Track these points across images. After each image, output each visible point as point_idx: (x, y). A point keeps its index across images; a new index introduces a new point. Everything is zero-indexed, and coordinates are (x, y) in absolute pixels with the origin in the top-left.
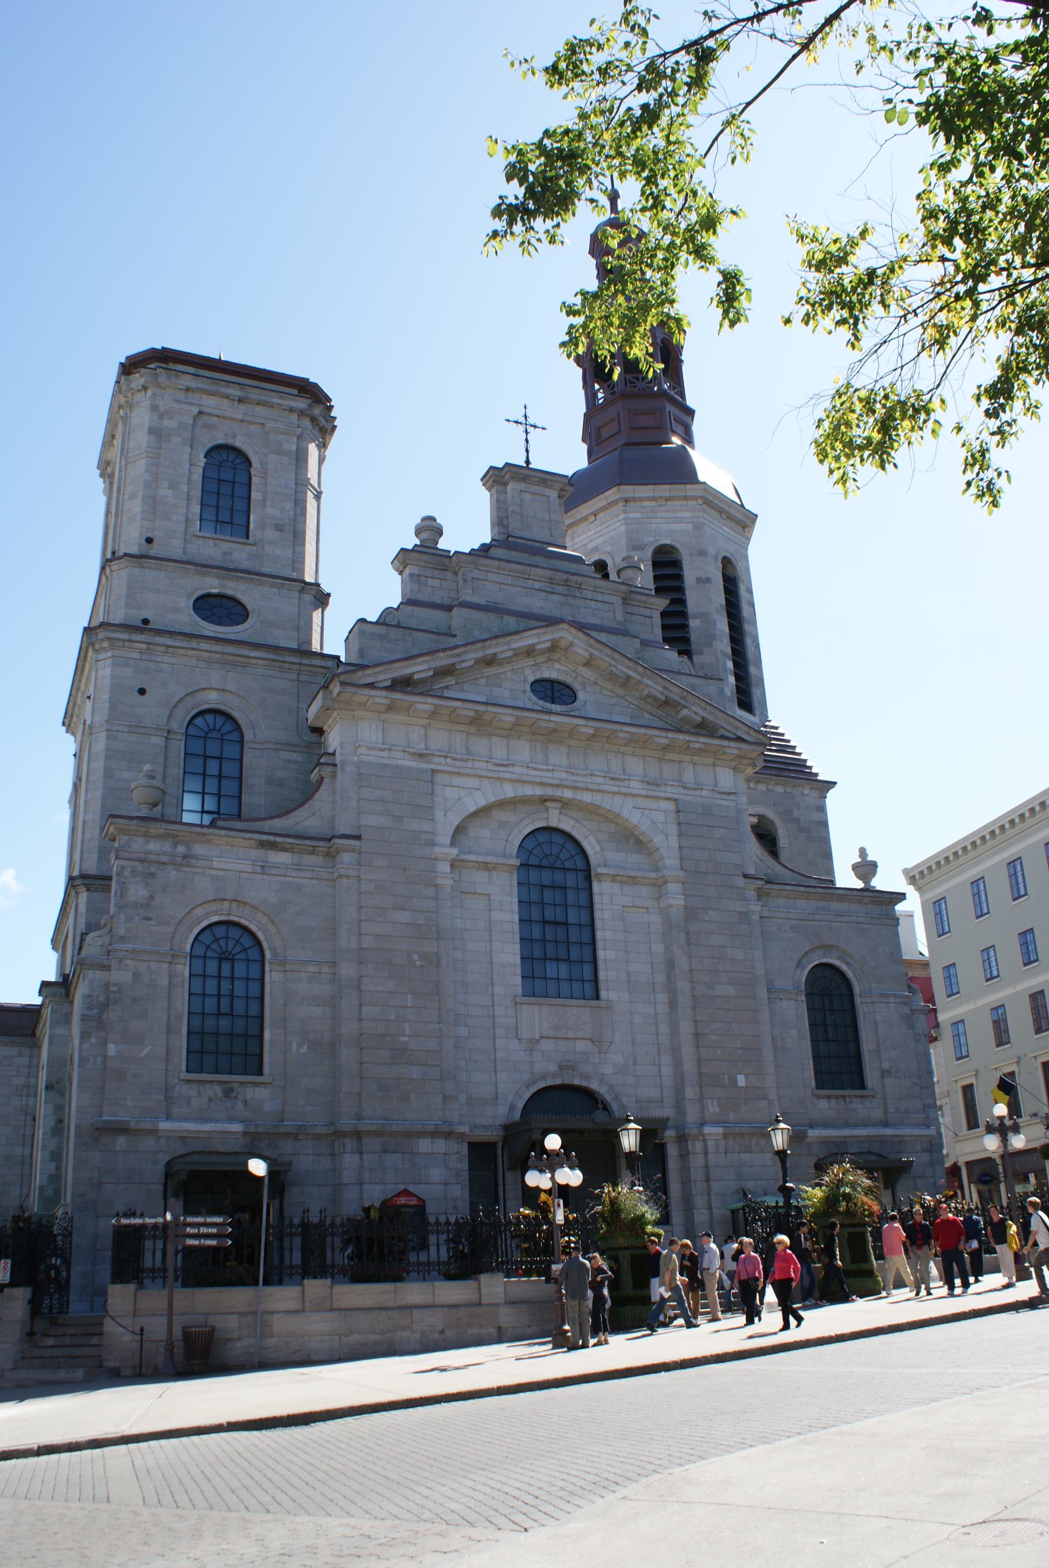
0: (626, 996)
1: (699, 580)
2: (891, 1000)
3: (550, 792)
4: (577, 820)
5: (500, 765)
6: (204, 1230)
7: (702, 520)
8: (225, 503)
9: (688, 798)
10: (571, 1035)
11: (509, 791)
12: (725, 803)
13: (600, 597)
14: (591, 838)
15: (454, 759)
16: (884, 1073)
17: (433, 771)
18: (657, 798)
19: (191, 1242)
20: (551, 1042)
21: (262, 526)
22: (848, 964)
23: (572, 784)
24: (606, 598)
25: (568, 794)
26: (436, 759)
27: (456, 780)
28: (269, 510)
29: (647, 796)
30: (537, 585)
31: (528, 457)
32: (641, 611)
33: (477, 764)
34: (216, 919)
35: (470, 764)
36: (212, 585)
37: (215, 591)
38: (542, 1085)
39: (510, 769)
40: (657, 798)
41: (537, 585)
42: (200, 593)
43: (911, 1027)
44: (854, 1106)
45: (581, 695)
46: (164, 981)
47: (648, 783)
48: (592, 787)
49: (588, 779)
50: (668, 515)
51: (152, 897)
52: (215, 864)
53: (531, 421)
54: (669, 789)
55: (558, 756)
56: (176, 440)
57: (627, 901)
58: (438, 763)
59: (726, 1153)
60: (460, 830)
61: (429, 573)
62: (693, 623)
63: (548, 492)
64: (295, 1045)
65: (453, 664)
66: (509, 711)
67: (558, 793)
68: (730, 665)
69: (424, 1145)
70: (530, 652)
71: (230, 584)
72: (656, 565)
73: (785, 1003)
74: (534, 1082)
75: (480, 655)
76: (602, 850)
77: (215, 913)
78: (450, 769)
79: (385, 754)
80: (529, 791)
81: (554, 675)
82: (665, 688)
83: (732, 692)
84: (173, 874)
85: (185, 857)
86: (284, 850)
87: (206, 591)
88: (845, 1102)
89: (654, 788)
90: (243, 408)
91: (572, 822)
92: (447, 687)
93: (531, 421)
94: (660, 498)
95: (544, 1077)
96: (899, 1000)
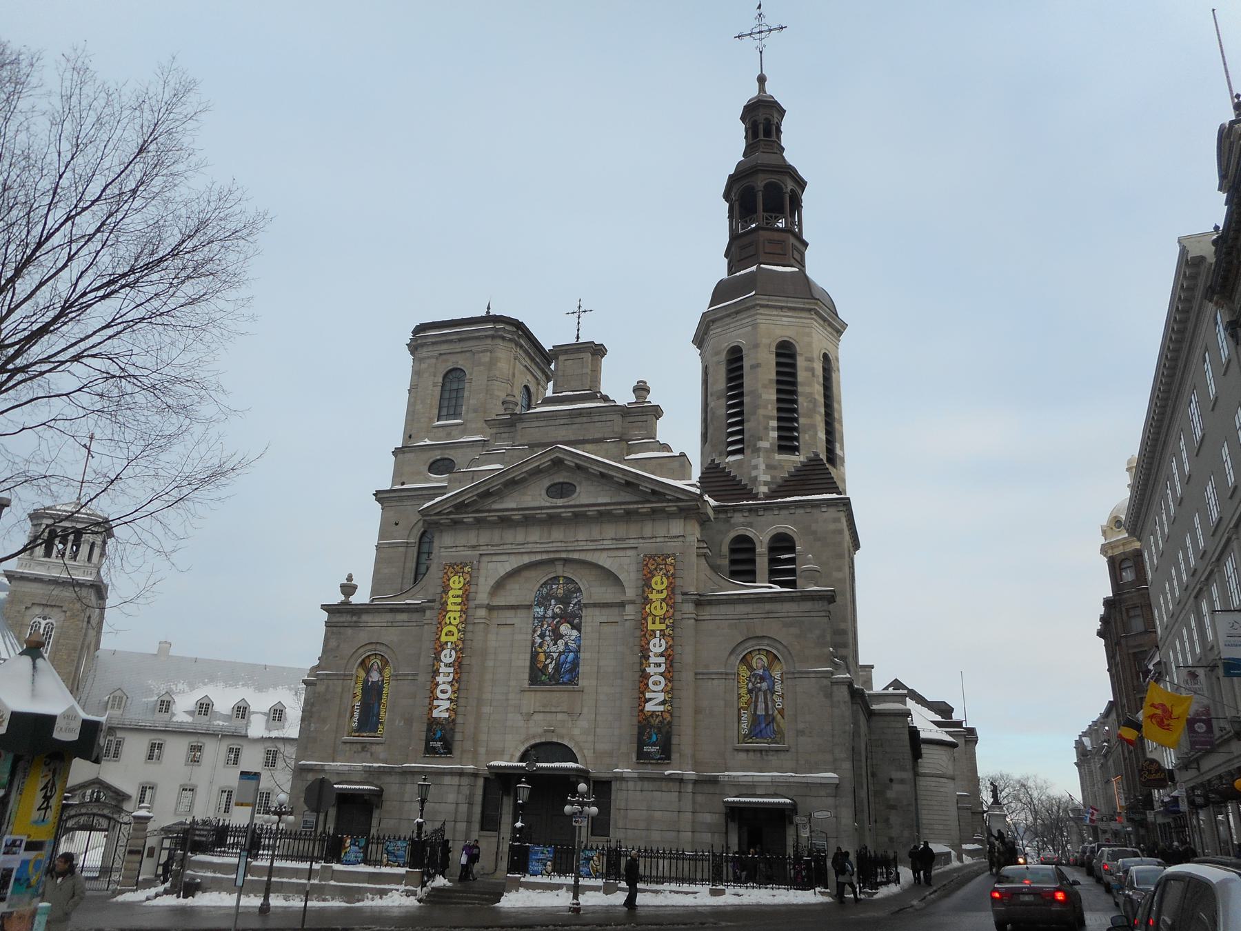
0: (594, 682)
2: (813, 675)
3: (552, 556)
5: (518, 544)
6: (202, 833)
8: (453, 402)
11: (526, 559)
13: (604, 418)
15: (493, 546)
16: (800, 733)
17: (481, 554)
19: (197, 838)
20: (542, 714)
21: (467, 412)
22: (777, 649)
23: (564, 549)
24: (609, 418)
25: (564, 555)
26: (482, 548)
27: (495, 558)
28: (471, 401)
29: (617, 549)
30: (562, 422)
31: (578, 335)
32: (640, 418)
34: (369, 653)
35: (501, 547)
36: (437, 455)
37: (439, 457)
38: (533, 742)
39: (526, 546)
41: (562, 422)
42: (431, 460)
43: (829, 695)
44: (770, 758)
45: (578, 489)
46: (339, 690)
47: (616, 540)
49: (576, 544)
50: (737, 324)
51: (338, 646)
52: (369, 624)
53: (576, 309)
54: (632, 541)
55: (557, 534)
56: (426, 375)
57: (604, 619)
58: (483, 550)
60: (499, 585)
61: (502, 430)
62: (746, 399)
63: (582, 355)
64: (397, 722)
65: (489, 489)
66: (517, 513)
68: (774, 423)
69: (447, 780)
70: (537, 472)
71: (447, 452)
72: (730, 362)
73: (715, 682)
74: (527, 740)
75: (502, 480)
78: (492, 552)
79: (454, 549)
80: (538, 557)
81: (561, 480)
83: (771, 444)
84: (349, 631)
85: (355, 622)
88: (762, 754)
90: (462, 344)
92: (494, 502)
93: (576, 309)
94: (732, 313)
95: (534, 737)
96: (819, 675)
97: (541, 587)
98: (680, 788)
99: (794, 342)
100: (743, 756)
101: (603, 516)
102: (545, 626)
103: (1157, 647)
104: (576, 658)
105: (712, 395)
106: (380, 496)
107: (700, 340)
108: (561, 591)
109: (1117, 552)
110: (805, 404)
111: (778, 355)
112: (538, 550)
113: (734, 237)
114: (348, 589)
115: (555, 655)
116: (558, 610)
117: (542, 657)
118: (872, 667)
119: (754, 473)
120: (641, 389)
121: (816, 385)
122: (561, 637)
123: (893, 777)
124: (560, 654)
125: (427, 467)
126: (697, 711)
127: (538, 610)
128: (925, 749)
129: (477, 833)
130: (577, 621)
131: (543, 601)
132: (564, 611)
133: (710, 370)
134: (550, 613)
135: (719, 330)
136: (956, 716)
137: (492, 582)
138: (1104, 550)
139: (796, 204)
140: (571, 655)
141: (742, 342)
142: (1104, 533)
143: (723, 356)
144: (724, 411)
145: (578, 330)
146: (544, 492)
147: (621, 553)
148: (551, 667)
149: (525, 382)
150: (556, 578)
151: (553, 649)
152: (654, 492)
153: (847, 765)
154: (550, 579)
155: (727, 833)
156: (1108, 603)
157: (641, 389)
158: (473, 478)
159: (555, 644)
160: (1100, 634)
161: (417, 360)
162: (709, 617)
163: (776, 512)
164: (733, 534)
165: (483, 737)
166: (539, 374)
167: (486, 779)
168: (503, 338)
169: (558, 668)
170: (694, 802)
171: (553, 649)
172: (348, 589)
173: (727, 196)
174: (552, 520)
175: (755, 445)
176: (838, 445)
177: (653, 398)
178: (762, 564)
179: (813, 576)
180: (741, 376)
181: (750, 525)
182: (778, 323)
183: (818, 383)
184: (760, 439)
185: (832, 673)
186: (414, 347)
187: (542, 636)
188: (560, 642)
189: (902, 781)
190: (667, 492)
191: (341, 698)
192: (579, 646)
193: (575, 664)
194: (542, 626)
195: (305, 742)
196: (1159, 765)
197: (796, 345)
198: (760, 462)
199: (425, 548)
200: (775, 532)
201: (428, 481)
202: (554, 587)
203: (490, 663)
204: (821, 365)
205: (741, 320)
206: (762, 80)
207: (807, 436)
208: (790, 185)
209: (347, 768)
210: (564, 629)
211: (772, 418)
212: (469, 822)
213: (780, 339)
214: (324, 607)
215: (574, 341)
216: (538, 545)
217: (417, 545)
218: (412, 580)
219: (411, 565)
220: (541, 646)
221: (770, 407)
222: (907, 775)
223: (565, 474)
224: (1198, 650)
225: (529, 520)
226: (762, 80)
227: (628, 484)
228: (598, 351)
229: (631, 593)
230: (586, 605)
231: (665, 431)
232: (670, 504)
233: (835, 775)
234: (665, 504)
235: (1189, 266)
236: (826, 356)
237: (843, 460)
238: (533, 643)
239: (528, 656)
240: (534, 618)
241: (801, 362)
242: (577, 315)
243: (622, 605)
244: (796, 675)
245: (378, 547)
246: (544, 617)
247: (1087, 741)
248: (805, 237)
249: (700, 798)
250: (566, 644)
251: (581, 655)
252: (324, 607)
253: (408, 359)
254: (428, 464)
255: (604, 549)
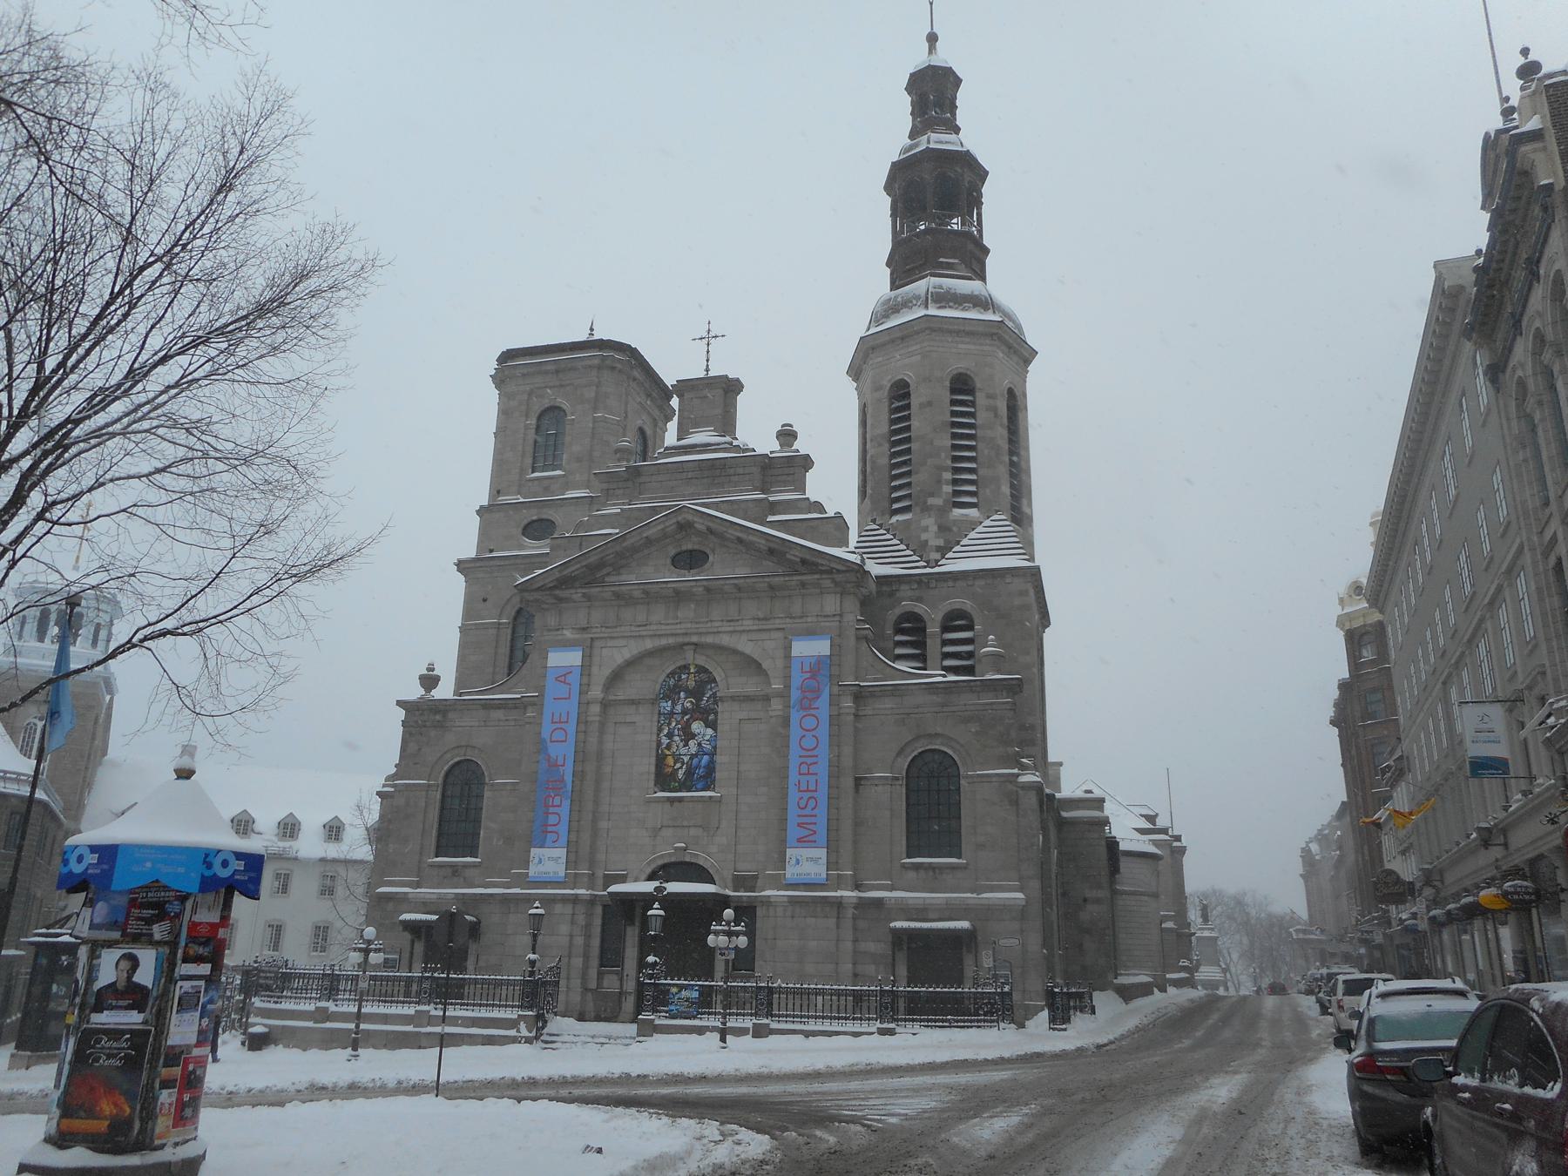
1: (922, 406)
3: (680, 640)
4: (707, 656)
5: (639, 626)
7: (928, 349)
9: (794, 626)
10: (685, 823)
11: (649, 644)
12: (827, 624)
14: (719, 669)
15: (607, 627)
17: (592, 638)
18: (770, 630)
20: (671, 830)
22: (952, 748)
23: (696, 631)
25: (695, 639)
26: (594, 630)
27: (610, 643)
29: (760, 630)
33: (623, 629)
35: (618, 629)
37: (535, 518)
39: (648, 627)
40: (770, 630)
42: (526, 522)
45: (711, 558)
48: (710, 630)
51: (420, 749)
53: (705, 334)
54: (777, 621)
55: (687, 612)
57: (744, 715)
59: (793, 917)
60: (616, 677)
62: (914, 446)
65: (602, 558)
67: (687, 640)
73: (880, 788)
76: (726, 676)
77: (457, 755)
80: (664, 642)
81: (690, 547)
82: (767, 540)
84: (433, 733)
86: (499, 708)
87: (529, 520)
89: (764, 622)
91: (704, 658)
92: (608, 574)
93: (705, 334)
96: (1002, 779)
97: (668, 676)
98: (838, 913)
99: (972, 375)
100: (911, 875)
101: (741, 591)
102: (674, 724)
103: (1399, 739)
104: (712, 763)
105: (872, 440)
106: (462, 566)
107: (855, 371)
108: (691, 684)
109: (1357, 624)
110: (986, 452)
111: (953, 391)
112: (663, 632)
113: (898, 243)
114: (430, 681)
115: (686, 759)
116: (688, 705)
117: (670, 761)
118: (1061, 764)
119: (924, 536)
120: (787, 435)
121: (999, 428)
122: (693, 736)
123: (1087, 896)
124: (692, 757)
125: (520, 530)
126: (858, 823)
127: (665, 704)
128: (1124, 864)
129: (596, 970)
130: (711, 717)
131: (671, 693)
132: (697, 705)
133: (869, 410)
134: (679, 708)
135: (880, 359)
136: (1161, 822)
137: (607, 672)
138: (1340, 622)
139: (976, 201)
140: (706, 758)
141: (909, 376)
142: (1341, 601)
143: (885, 393)
144: (887, 460)
145: (708, 361)
146: (669, 561)
147: (764, 636)
148: (681, 774)
149: (639, 422)
150: (685, 668)
151: (683, 751)
152: (804, 562)
153: (1035, 884)
154: (679, 668)
155: (894, 965)
156: (1344, 686)
157: (787, 435)
158: (581, 545)
159: (686, 745)
160: (1333, 723)
161: (504, 396)
162: (870, 713)
163: (951, 584)
164: (898, 611)
165: (601, 857)
166: (656, 413)
167: (605, 907)
168: (613, 368)
169: (690, 773)
170: (855, 929)
171: (683, 751)
172: (430, 681)
173: (889, 188)
174: (679, 597)
175: (925, 502)
176: (1025, 501)
177: (801, 446)
178: (934, 647)
179: (997, 661)
180: (908, 418)
181: (919, 599)
182: (954, 350)
183: (1001, 425)
184: (932, 495)
185: (1018, 775)
186: (499, 380)
187: (670, 735)
188: (691, 743)
189: (1098, 901)
190: (820, 561)
191: (425, 812)
192: (715, 748)
193: (711, 769)
194: (669, 724)
195: (383, 865)
196: (1398, 877)
197: (976, 379)
198: (930, 522)
199: (521, 631)
200: (949, 608)
201: (521, 547)
202: (683, 677)
203: (607, 769)
204: (1005, 403)
205: (908, 347)
206: (932, 39)
207: (988, 491)
208: (968, 177)
209: (435, 896)
210: (696, 727)
211: (946, 470)
212: (586, 957)
213: (955, 372)
214: (400, 703)
215: (702, 374)
216: (663, 627)
217: (511, 626)
218: (506, 671)
219: (504, 650)
220: (669, 747)
221: (943, 455)
222: (1103, 893)
223: (695, 539)
224: (1445, 744)
225: (650, 596)
226: (932, 39)
227: (771, 552)
228: (731, 387)
229: (777, 686)
230: (722, 699)
231: (817, 486)
232: (824, 576)
233: (1020, 895)
234: (816, 576)
235: (1445, 298)
236: (1011, 392)
237: (1030, 519)
238: (659, 744)
239: (653, 760)
240: (660, 714)
241: (981, 399)
242: (705, 341)
243: (767, 699)
244: (975, 780)
245: (463, 629)
246: (672, 713)
247: (1314, 847)
248: (986, 242)
249: (862, 924)
250: (699, 744)
251: (718, 758)
252: (400, 703)
253: (493, 395)
254: (522, 525)
255: (744, 631)
